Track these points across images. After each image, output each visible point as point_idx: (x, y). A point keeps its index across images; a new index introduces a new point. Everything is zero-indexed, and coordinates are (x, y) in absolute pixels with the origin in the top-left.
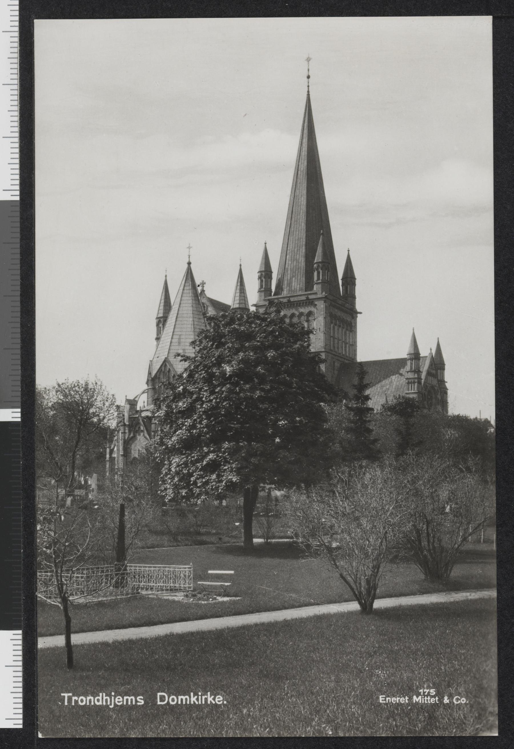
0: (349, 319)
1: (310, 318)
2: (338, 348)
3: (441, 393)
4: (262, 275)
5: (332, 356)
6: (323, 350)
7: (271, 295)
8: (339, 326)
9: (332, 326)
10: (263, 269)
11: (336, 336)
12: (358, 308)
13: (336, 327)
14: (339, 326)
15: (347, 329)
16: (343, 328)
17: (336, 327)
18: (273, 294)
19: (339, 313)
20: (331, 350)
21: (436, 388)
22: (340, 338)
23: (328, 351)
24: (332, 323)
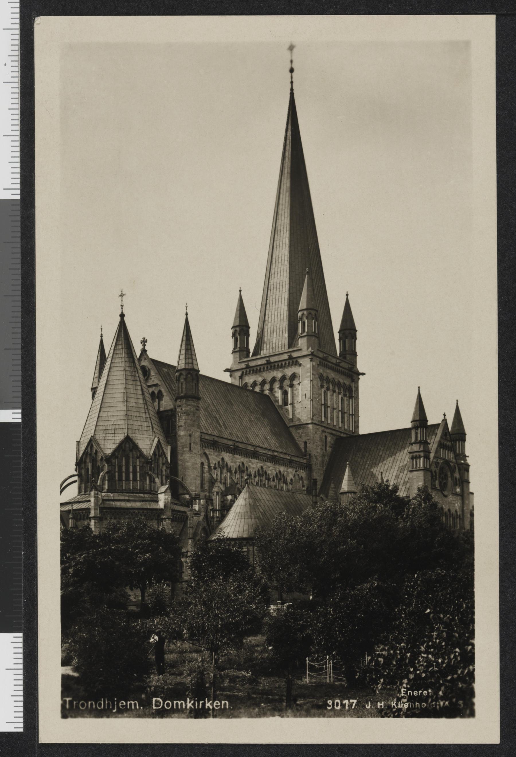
0: (347, 382)
1: (295, 382)
2: (332, 419)
3: (460, 469)
4: (235, 331)
5: (323, 428)
6: (310, 421)
7: (248, 356)
8: (334, 391)
9: (323, 390)
10: (237, 324)
11: (329, 404)
12: (360, 367)
13: (328, 392)
14: (334, 391)
15: (345, 395)
16: (339, 393)
17: (329, 393)
18: (251, 354)
19: (332, 375)
20: (322, 422)
21: (452, 464)
22: (335, 406)
23: (316, 422)
24: (322, 387)
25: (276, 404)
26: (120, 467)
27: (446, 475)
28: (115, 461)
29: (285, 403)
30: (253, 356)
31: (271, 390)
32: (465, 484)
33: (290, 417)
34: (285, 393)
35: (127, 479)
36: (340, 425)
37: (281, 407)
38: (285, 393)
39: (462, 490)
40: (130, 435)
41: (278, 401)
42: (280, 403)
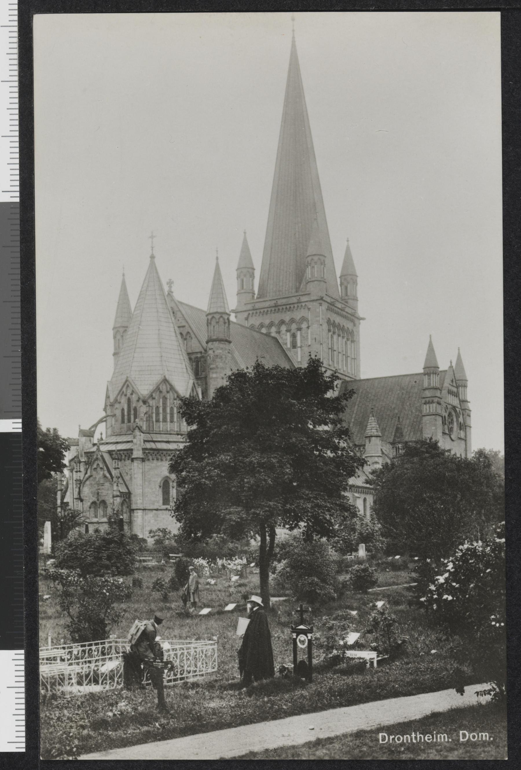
25: (284, 347)
26: (157, 408)
27: (452, 420)
28: (151, 402)
29: (294, 346)
30: (257, 298)
31: (279, 332)
32: (468, 429)
33: (299, 360)
34: (294, 336)
35: (165, 420)
36: (345, 368)
37: (289, 349)
38: (294, 336)
39: (466, 436)
40: (167, 377)
41: (286, 344)
42: (289, 346)
